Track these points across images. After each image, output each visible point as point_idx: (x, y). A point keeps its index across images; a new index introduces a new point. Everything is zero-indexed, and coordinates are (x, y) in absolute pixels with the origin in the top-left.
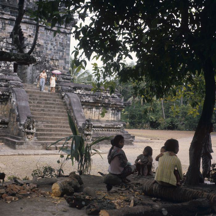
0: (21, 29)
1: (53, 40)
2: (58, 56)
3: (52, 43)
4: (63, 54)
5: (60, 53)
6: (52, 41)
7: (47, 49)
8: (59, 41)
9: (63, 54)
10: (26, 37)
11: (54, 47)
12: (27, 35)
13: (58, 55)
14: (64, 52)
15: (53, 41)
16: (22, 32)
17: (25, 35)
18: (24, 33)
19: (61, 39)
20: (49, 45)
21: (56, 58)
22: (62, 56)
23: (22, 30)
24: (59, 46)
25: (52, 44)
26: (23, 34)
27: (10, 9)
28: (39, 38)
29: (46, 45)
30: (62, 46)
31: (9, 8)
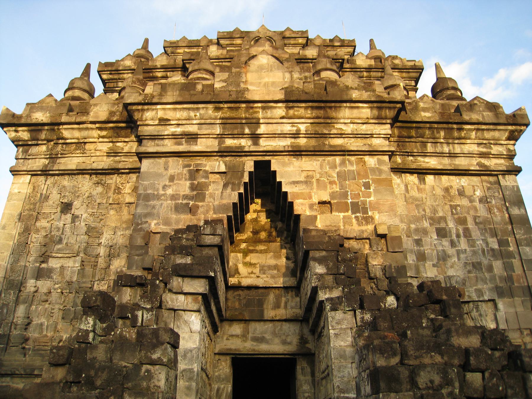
0: (280, 183)
1: (441, 214)
2: (484, 281)
3: (443, 225)
4: (508, 267)
5: (490, 268)
6: (441, 218)
7: (422, 257)
8: (472, 213)
9: (508, 267)
10: (308, 213)
11: (453, 244)
12: (311, 206)
13: (487, 275)
14: (510, 255)
15: (444, 219)
16: (286, 193)
17: (301, 208)
18: (297, 196)
19: (477, 204)
20: (428, 240)
21: (480, 292)
22: (509, 279)
23: (285, 188)
24: (476, 233)
25: (444, 229)
26: (292, 204)
27: (219, 114)
28: (373, 209)
29: (418, 242)
30: (494, 234)
31: (217, 109)
